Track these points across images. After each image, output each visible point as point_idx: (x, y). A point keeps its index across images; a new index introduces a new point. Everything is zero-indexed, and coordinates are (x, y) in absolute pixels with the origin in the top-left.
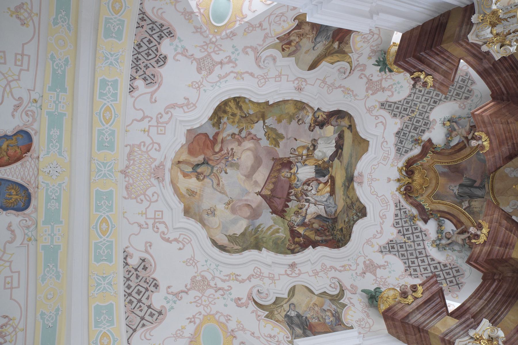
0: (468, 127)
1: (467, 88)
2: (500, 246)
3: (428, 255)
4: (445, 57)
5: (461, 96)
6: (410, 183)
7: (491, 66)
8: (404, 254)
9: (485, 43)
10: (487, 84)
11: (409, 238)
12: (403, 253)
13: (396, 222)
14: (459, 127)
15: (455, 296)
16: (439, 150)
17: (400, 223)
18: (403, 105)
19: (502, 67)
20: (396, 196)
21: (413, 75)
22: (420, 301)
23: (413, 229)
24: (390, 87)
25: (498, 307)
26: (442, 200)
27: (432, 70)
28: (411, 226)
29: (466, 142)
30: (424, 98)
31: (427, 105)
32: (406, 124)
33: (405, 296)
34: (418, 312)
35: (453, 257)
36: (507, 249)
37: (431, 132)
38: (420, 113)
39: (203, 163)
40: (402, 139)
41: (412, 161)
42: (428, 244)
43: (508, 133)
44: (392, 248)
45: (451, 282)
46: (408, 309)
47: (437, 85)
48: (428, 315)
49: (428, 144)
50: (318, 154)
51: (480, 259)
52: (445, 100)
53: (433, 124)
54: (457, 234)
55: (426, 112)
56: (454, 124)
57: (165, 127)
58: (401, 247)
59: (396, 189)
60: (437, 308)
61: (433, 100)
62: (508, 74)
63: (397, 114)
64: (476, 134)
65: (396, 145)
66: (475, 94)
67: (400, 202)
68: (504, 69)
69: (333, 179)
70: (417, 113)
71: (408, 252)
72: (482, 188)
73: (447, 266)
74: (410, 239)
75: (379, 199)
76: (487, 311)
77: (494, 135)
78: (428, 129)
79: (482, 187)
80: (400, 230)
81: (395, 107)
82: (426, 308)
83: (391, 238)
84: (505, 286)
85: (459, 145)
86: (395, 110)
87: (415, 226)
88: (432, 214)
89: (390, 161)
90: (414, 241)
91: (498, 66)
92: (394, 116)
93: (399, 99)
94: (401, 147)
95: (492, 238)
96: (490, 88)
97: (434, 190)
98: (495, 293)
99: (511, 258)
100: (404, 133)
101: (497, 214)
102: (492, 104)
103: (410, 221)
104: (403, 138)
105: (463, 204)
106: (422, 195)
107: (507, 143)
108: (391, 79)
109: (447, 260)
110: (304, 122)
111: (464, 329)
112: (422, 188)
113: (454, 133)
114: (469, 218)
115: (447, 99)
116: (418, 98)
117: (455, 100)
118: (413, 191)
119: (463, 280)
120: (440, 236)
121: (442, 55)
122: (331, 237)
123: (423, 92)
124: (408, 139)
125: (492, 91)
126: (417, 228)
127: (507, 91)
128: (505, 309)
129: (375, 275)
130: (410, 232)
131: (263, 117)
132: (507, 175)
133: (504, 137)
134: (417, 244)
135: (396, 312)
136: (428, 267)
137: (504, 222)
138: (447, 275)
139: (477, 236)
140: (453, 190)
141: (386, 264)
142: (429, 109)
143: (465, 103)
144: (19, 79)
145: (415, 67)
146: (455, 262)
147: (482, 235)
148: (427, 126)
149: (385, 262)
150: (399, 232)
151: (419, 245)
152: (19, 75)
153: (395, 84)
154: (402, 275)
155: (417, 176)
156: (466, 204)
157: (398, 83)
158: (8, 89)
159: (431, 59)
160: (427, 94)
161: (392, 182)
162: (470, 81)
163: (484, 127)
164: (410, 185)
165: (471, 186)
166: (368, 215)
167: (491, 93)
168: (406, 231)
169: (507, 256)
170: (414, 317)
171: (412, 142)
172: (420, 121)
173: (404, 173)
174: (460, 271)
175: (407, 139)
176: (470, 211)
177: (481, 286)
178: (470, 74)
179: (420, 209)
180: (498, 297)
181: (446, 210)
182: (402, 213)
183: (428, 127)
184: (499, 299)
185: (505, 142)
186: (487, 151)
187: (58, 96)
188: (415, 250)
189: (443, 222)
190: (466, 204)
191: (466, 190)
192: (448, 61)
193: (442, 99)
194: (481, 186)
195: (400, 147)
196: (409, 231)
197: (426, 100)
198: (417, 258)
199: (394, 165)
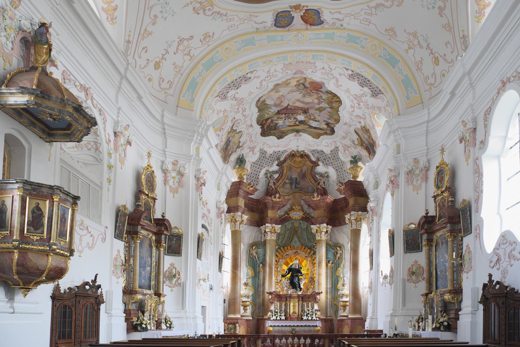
42: (267, 168)
50: (312, 121)
51: (266, 200)
58: (264, 157)
65: (316, 150)
69: (298, 125)
83: (267, 152)
89: (308, 147)
90: (267, 162)
144: (355, 19)
150: (271, 154)
151: (266, 164)
152: (357, 19)
155: (300, 159)
156: (287, 181)
158: (349, 15)
165: (296, 183)
173: (302, 153)
187: (344, 37)
188: (263, 163)
190: (287, 181)
191: (294, 181)
198: (259, 165)
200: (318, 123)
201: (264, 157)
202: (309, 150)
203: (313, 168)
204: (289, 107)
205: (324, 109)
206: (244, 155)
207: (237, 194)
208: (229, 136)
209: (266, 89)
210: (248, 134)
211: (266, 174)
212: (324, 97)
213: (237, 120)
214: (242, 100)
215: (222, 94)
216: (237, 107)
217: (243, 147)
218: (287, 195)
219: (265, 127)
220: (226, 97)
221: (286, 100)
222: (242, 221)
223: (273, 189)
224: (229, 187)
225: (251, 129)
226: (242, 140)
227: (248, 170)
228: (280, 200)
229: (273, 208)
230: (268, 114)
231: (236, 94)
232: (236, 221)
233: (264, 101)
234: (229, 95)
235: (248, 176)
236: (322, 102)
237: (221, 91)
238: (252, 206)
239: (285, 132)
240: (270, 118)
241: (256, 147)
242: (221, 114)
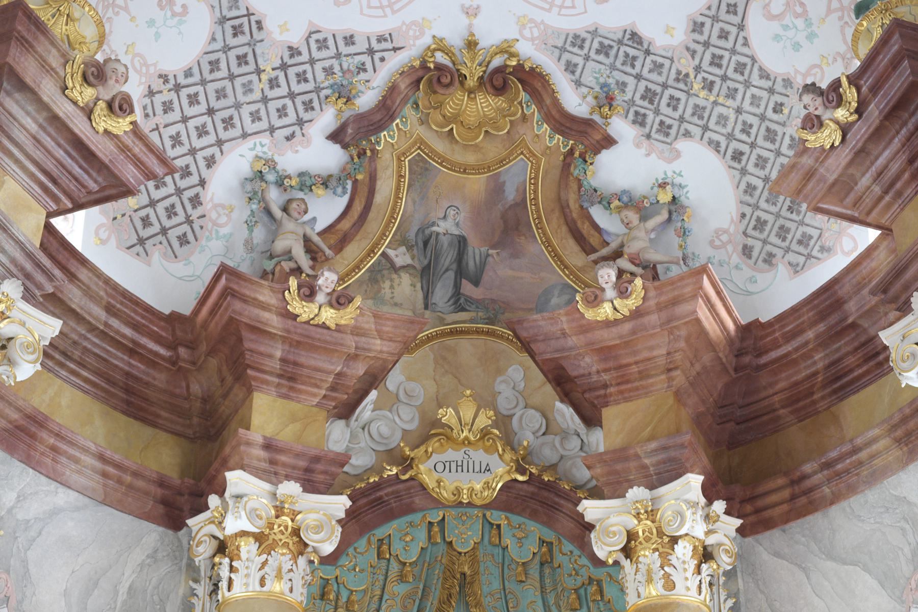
0: (653, 256)
1: (779, 253)
2: (283, 360)
3: (226, 147)
4: (899, 185)
5: (756, 234)
6: (462, 84)
7: (850, 320)
8: (219, 69)
10: (794, 311)
11: (273, 83)
12: (223, 65)
13: (325, 40)
14: (653, 230)
15: (104, 236)
16: (576, 173)
17: (324, 54)
18: (733, 51)
19: (843, 351)
20: (416, 38)
21: (850, 83)
22: (79, 126)
23: (306, 98)
24: (799, 10)
25: (90, 360)
26: (410, 186)
27: (860, 145)
28: (318, 90)
29: (605, 252)
30: (755, 121)
31: (729, 129)
32: (667, 63)
33: (91, 79)
34: (41, 121)
35: (226, 224)
36: (276, 380)
37: (638, 145)
38: (704, 108)
40: (613, 52)
41: (538, 85)
42: (262, 145)
43: (640, 372)
44: (234, 27)
45: (146, 222)
46: (48, 90)
47: (807, 161)
48: (38, 155)
49: (598, 137)
51: (238, 305)
52: (743, 186)
53: (662, 152)
54: (305, 236)
55: (706, 128)
56: (665, 215)
58: (242, 60)
59: (440, 34)
60: (65, 180)
61: (746, 148)
62: (820, 365)
63: (701, 33)
64: (638, 282)
65: (594, 33)
66: (759, 276)
67: (395, 49)
68: (837, 356)
70: (702, 98)
71: (227, 83)
72: (455, 303)
73: (194, 207)
74: (271, 88)
76: (74, 330)
77: (633, 332)
78: (648, 136)
79: (459, 302)
80: (300, 53)
81: (727, 27)
82: (59, 145)
83: (268, 24)
84: (160, 379)
85: (593, 232)
86: (717, 26)
87: (316, 104)
88: (362, 154)
89: (539, 16)
90: (265, 100)
91: (847, 339)
92: (695, 23)
93: (754, 41)
94: (586, 51)
95: (308, 337)
96: (781, 318)
97: (443, 161)
98: (133, 351)
99: (250, 391)
100: (634, 58)
101: (385, 349)
102: (731, 326)
103: (331, 86)
104: (616, 56)
105: (403, 249)
106: (423, 122)
107: (606, 370)
108: (829, 11)
109: (216, 206)
111: (16, 266)
112: (447, 120)
113: (633, 216)
114: (358, 267)
115: (746, 192)
116: (755, 100)
117: (743, 215)
118: (435, 92)
119: (156, 256)
120: (293, 183)
121: (907, 175)
123: (775, 117)
124: (615, 73)
125: (770, 324)
126: (313, 109)
127: (765, 365)
128: (86, 380)
130: (297, 88)
132: (500, 371)
133: (624, 361)
134: (258, 111)
135: (32, 47)
136: (184, 149)
137: (359, 369)
138: (167, 209)
139: (309, 292)
140: (445, 217)
141: (178, 9)
142: (716, 137)
143: (730, 248)
145: (875, 89)
146: (211, 233)
147: (314, 308)
148: (658, 131)
149: (184, 6)
150: (294, 51)
151: (256, 117)
153: (809, 24)
154: (145, 64)
156: (401, 257)
157: (811, 36)
159: (896, 143)
160: (768, 130)
161: (465, 21)
162: (802, 259)
163: (658, 304)
164: (457, 83)
165: (461, 272)
167: (763, 320)
168: (298, 75)
169: (255, 379)
170: (23, 108)
171: (603, 86)
172: (675, 109)
173: (497, 62)
174: (184, 248)
175: (613, 67)
176: (380, 271)
177: (148, 309)
178: (825, 260)
179: (378, 117)
180: (120, 360)
181: (378, 198)
182: (358, 59)
183: (653, 134)
184: (116, 362)
185: (611, 364)
186: (583, 315)
188: (238, 106)
189: (339, 190)
190: (401, 257)
191: (448, 258)
192: (886, 192)
193: (748, 178)
194: (462, 300)
195: (587, 45)
196: (299, 82)
197: (746, 129)
198: (211, 112)
199: (523, 26)
228: (347, 316)
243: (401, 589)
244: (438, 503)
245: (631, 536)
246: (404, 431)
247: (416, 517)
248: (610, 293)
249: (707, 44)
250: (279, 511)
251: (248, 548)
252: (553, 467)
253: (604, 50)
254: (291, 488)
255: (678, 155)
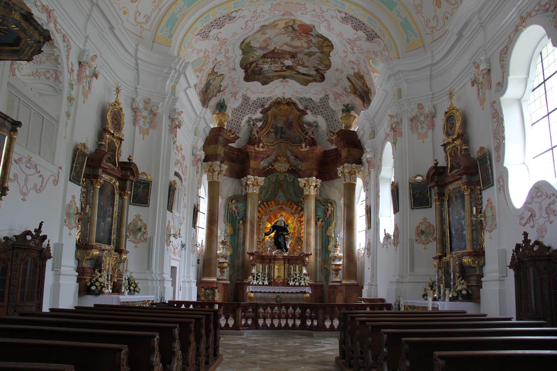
2: (254, 156)
9: (344, 167)
10: (332, 150)
28: (258, 106)
37: (311, 115)
39: (294, 29)
42: (250, 115)
50: (300, 67)
55: (322, 114)
57: (317, 17)
58: (246, 104)
65: (304, 98)
69: (285, 71)
70: (321, 110)
75: (273, 90)
78: (313, 114)
79: (281, 137)
83: (251, 98)
90: (250, 109)
96: (330, 150)
99: (250, 160)
106: (276, 109)
110: (318, 65)
114: (265, 132)
116: (330, 112)
122: (250, 75)
125: (328, 151)
129: (231, 97)
131: (321, 53)
139: (258, 147)
149: (238, 99)
150: (255, 101)
151: (249, 111)
155: (286, 107)
156: (272, 130)
165: (282, 132)
166: (263, 86)
171: (306, 105)
173: (288, 100)
181: (268, 121)
188: (246, 110)
197: (328, 116)
198: (242, 112)
200: (307, 69)
201: (246, 104)
202: (296, 98)
203: (300, 117)
204: (276, 51)
205: (314, 54)
206: (225, 100)
207: (216, 142)
208: (210, 78)
209: (251, 31)
210: (230, 78)
211: (248, 122)
212: (314, 40)
213: (219, 62)
214: (225, 41)
215: (204, 33)
216: (219, 48)
217: (224, 91)
218: (271, 145)
219: (249, 71)
220: (207, 37)
221: (272, 43)
222: (221, 171)
223: (256, 138)
224: (208, 133)
225: (233, 73)
226: (224, 84)
227: (229, 117)
229: (256, 158)
230: (252, 57)
231: (219, 34)
232: (214, 171)
233: (249, 43)
234: (211, 34)
235: (229, 123)
236: (312, 46)
237: (202, 29)
238: (232, 155)
239: (271, 77)
240: (255, 61)
241: (238, 92)
242: (202, 54)
243: (272, 186)
244: (277, 172)
245: (305, 184)
246: (273, 159)
247: (274, 174)
248: (304, 147)
249: (322, 102)
250: (255, 180)
251: (251, 186)
252: (295, 166)
253: (306, 100)
254: (256, 177)
255: (317, 117)
